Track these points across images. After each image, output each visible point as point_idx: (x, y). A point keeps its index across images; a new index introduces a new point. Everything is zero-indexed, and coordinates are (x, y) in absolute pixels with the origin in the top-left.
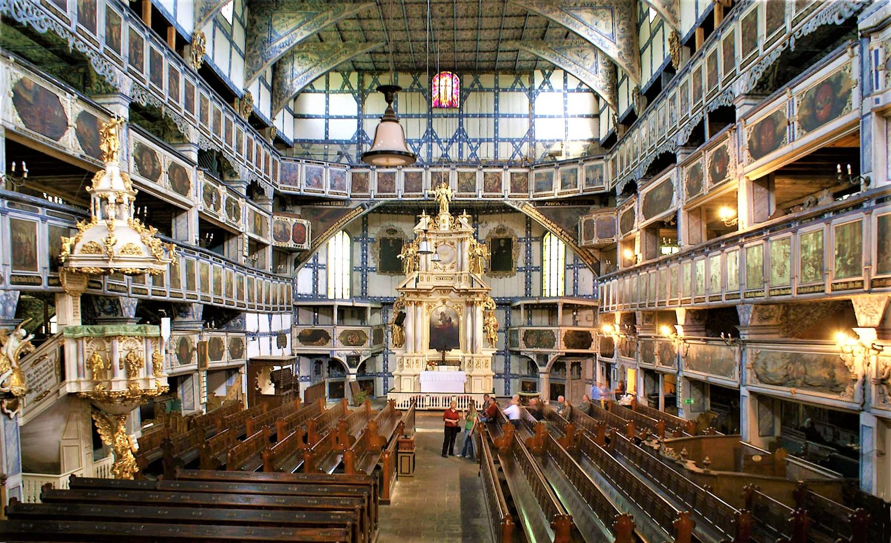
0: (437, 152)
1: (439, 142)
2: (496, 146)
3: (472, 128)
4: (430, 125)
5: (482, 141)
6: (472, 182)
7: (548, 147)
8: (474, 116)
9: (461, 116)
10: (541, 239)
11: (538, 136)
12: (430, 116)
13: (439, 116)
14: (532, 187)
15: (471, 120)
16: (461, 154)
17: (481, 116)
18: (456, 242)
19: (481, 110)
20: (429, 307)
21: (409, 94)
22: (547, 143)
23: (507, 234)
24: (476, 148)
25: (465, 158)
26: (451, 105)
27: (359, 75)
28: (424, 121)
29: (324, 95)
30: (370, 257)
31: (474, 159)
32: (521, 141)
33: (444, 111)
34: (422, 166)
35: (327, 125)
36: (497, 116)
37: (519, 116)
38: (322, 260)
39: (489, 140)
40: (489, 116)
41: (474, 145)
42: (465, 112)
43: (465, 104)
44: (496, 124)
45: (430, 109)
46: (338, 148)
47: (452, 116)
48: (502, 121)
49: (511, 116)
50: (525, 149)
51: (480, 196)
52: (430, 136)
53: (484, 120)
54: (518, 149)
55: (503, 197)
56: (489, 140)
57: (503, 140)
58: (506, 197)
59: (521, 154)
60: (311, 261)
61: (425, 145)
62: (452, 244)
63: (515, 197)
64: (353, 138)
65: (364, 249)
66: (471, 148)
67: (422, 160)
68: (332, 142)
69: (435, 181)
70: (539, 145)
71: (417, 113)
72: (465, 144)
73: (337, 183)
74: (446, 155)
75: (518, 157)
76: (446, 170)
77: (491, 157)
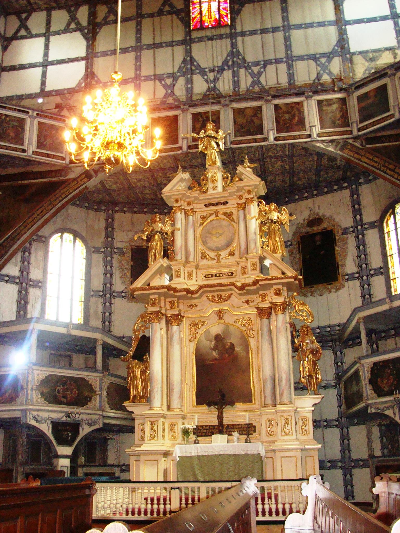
0: (200, 86)
1: (203, 72)
2: (290, 67)
3: (251, 49)
4: (189, 52)
5: (267, 63)
6: (256, 121)
7: (372, 60)
8: (253, 33)
9: (233, 36)
10: (379, 225)
11: (355, 46)
12: (187, 42)
13: (201, 40)
14: (354, 115)
15: (248, 39)
16: (236, 84)
17: (264, 31)
18: (234, 211)
19: (262, 23)
20: (195, 325)
21: (157, 19)
22: (371, 55)
23: (325, 225)
24: (260, 73)
25: (243, 87)
26: (218, 24)
27: (90, 9)
28: (179, 52)
29: (42, 40)
30: (117, 274)
31: (257, 89)
32: (329, 56)
33: (209, 33)
34: (178, 107)
35: (44, 74)
36: (287, 28)
37: (322, 24)
38: (35, 274)
39: (278, 61)
40: (275, 30)
41: (256, 69)
42: (239, 29)
43: (238, 21)
44: (287, 39)
45: (188, 33)
46: (58, 100)
47: (220, 37)
48: (297, 35)
49: (310, 26)
50: (336, 66)
51: (271, 138)
52: (190, 67)
53: (269, 37)
54: (325, 68)
55: (309, 136)
56: (278, 61)
57: (301, 58)
58: (315, 135)
59: (330, 73)
60: (12, 269)
61: (181, 81)
62: (229, 215)
63: (329, 134)
64: (79, 84)
65: (108, 264)
66: (252, 75)
67: (177, 100)
68: (50, 94)
69: (198, 125)
70: (358, 59)
71: (169, 39)
72: (242, 71)
73: (48, 142)
74: (215, 89)
75: (326, 78)
76: (215, 108)
77: (284, 81)
